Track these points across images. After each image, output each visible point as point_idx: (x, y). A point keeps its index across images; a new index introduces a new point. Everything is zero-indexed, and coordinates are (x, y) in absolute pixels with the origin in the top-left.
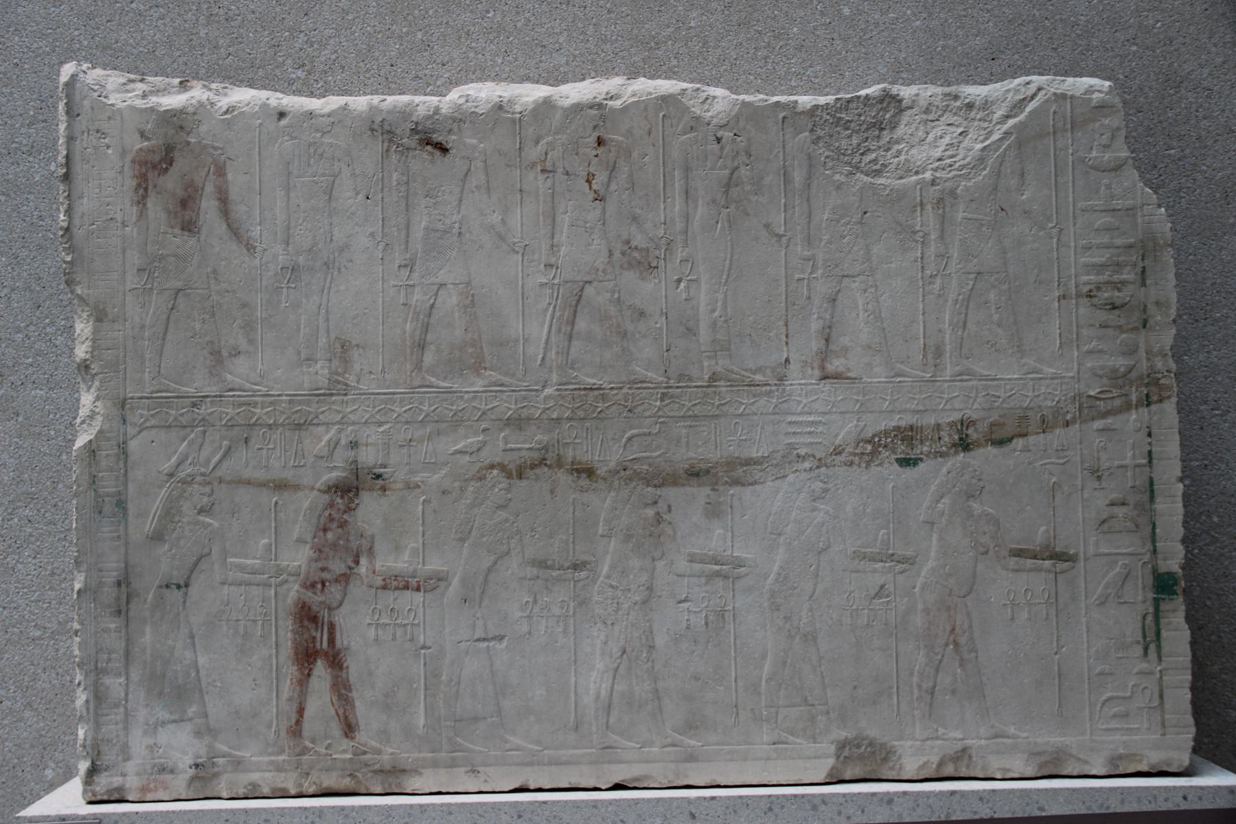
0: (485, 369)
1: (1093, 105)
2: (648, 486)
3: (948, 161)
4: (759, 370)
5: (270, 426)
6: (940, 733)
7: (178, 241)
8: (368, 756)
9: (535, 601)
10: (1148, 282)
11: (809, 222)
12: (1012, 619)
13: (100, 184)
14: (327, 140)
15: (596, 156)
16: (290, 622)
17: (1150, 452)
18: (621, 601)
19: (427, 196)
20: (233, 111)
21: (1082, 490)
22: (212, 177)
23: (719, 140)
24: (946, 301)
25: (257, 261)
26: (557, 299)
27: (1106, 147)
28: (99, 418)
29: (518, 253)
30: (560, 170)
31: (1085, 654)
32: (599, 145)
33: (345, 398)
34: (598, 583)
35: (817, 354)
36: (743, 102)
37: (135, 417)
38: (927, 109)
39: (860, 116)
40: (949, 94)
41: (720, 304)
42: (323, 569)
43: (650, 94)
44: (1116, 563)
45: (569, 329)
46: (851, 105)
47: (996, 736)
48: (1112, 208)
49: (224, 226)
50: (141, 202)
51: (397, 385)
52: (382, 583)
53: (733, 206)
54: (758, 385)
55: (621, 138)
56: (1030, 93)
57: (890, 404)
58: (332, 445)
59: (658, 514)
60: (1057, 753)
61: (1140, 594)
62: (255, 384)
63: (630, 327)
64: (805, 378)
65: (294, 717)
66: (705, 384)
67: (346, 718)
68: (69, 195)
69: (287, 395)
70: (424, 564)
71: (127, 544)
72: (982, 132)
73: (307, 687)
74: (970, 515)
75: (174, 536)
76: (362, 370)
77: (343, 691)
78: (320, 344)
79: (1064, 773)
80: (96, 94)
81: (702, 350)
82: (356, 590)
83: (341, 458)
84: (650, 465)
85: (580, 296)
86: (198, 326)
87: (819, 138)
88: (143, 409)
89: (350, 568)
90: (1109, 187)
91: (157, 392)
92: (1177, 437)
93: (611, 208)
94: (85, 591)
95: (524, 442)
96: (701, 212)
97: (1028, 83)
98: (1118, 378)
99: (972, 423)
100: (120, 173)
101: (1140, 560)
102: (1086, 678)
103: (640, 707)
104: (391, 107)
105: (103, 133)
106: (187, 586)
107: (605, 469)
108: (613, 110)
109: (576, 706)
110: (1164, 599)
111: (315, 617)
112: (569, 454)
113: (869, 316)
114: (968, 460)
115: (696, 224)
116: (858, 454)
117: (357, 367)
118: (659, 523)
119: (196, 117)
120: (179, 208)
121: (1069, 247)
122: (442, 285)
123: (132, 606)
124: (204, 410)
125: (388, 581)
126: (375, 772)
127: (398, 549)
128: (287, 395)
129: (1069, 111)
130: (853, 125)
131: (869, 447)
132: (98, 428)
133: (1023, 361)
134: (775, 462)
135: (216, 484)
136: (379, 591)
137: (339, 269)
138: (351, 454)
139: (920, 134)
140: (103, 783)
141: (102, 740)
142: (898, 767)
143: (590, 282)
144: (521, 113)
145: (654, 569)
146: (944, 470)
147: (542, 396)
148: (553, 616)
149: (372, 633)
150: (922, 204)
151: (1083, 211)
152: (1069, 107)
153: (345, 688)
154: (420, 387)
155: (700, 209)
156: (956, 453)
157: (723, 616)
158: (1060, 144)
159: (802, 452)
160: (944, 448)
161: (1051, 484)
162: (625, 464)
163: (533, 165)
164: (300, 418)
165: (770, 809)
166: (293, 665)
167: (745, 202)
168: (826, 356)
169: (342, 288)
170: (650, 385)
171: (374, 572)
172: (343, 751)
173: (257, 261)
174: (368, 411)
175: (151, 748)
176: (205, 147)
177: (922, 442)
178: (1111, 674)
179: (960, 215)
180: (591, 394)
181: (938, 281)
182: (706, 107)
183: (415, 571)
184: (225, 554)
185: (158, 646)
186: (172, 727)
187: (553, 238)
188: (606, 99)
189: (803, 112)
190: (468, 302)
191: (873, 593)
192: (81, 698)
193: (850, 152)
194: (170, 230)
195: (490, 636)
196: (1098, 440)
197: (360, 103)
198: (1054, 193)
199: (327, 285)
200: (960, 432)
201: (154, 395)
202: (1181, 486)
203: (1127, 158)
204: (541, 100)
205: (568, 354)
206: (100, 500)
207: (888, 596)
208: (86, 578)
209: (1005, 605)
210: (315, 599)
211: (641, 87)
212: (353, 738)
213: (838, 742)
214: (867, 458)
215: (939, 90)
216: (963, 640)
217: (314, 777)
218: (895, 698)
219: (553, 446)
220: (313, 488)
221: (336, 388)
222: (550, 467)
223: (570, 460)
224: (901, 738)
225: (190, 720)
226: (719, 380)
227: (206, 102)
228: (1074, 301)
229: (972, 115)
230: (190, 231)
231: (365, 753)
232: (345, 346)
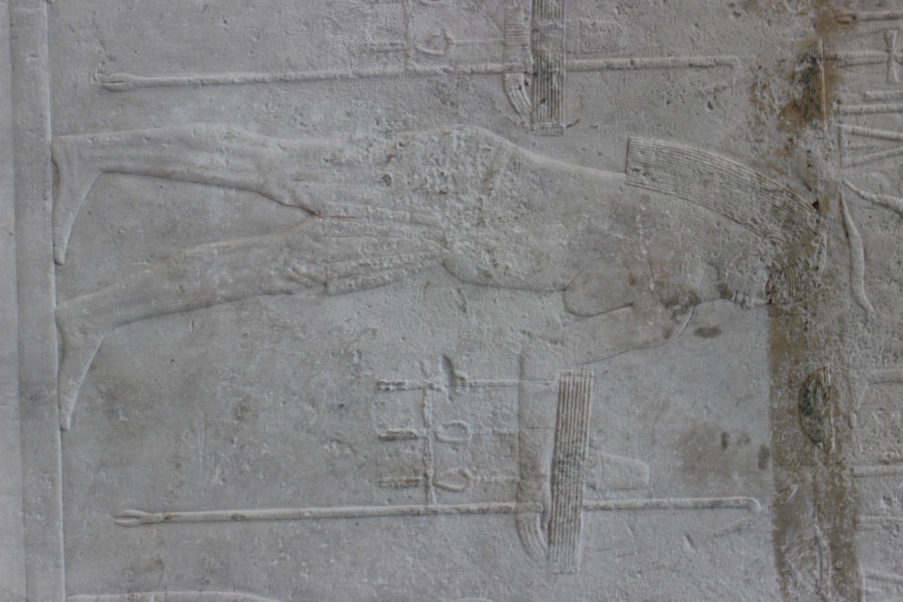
18: (451, 202)
34: (498, 138)
59: (695, 301)
84: (831, 276)
107: (818, 152)
109: (162, 85)
118: (667, 305)
145: (538, 291)
148: (407, 17)
162: (834, 203)
223: (842, 53)
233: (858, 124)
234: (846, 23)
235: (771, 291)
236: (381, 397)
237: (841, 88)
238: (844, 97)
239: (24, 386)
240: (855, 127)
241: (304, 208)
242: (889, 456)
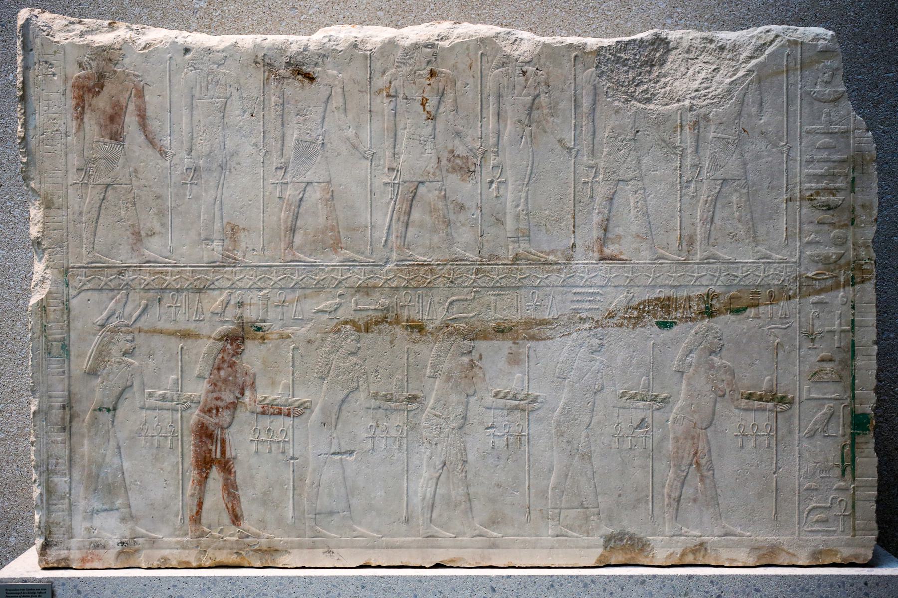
0: (341, 248)
1: (818, 50)
2: (465, 339)
3: (703, 92)
4: (552, 252)
5: (177, 290)
6: (683, 531)
7: (107, 147)
8: (250, 539)
9: (377, 426)
10: (856, 189)
11: (594, 138)
12: (742, 447)
13: (48, 104)
14: (221, 70)
15: (429, 85)
16: (192, 438)
17: (853, 321)
18: (442, 426)
19: (298, 114)
20: (149, 47)
21: (799, 349)
22: (133, 98)
23: (524, 73)
24: (699, 201)
25: (168, 163)
26: (397, 195)
27: (827, 83)
28: (49, 282)
29: (367, 159)
30: (401, 95)
31: (797, 474)
32: (431, 76)
33: (234, 269)
34: (426, 413)
35: (597, 241)
37: (75, 282)
38: (689, 49)
39: (635, 55)
40: (706, 39)
41: (523, 200)
42: (217, 399)
43: (472, 36)
44: (823, 405)
45: (406, 218)
46: (629, 47)
47: (726, 535)
48: (830, 131)
49: (143, 137)
50: (80, 117)
51: (274, 260)
52: (262, 409)
53: (534, 125)
54: (551, 264)
55: (448, 71)
56: (769, 39)
57: (653, 279)
58: (224, 305)
59: (472, 360)
60: (772, 548)
61: (840, 429)
62: (166, 258)
63: (453, 217)
64: (587, 259)
65: (195, 509)
67: (234, 510)
68: (25, 112)
69: (190, 266)
70: (293, 396)
71: (70, 377)
72: (731, 69)
73: (205, 487)
74: (712, 367)
75: (105, 372)
76: (247, 247)
77: (232, 490)
78: (215, 227)
79: (777, 563)
80: (45, 34)
81: (509, 235)
82: (242, 414)
83: (232, 313)
84: (466, 324)
85: (415, 193)
86: (123, 213)
87: (603, 72)
88: (81, 275)
89: (238, 398)
90: (828, 114)
91: (92, 263)
92: (874, 310)
93: (440, 124)
94: (39, 412)
95: (370, 304)
96: (509, 129)
97: (768, 31)
98: (829, 263)
99: (715, 296)
100: (63, 94)
101: (842, 403)
102: (797, 492)
103: (456, 506)
104: (270, 45)
105: (51, 64)
106: (115, 409)
108: (443, 49)
109: (407, 506)
110: (859, 434)
111: (211, 434)
112: (405, 314)
113: (638, 212)
114: (712, 324)
115: (505, 139)
116: (627, 318)
117: (243, 245)
118: (473, 368)
119: (121, 52)
120: (108, 122)
121: (796, 161)
122: (309, 184)
123: (74, 424)
124: (128, 277)
125: (266, 408)
126: (256, 551)
127: (274, 384)
128: (190, 266)
129: (799, 54)
130: (629, 62)
131: (636, 313)
132: (47, 290)
133: (757, 249)
134: (562, 323)
135: (136, 333)
136: (259, 415)
137: (230, 170)
138: (239, 311)
139: (682, 69)
140: (54, 554)
141: (53, 523)
142: (650, 555)
143: (423, 183)
145: (468, 403)
146: (693, 332)
147: (385, 270)
148: (391, 437)
149: (253, 447)
150: (681, 126)
151: (808, 133)
152: (799, 51)
153: (233, 488)
154: (291, 261)
155: (509, 127)
156: (703, 319)
157: (520, 440)
158: (792, 80)
159: (584, 315)
160: (693, 315)
161: (776, 344)
162: (447, 322)
163: (380, 91)
164: (200, 284)
165: (552, 586)
166: (194, 470)
168: (604, 242)
169: (233, 185)
170: (467, 262)
171: (256, 402)
172: (232, 534)
173: (168, 163)
174: (251, 279)
175: (88, 530)
176: (128, 75)
177: (676, 310)
178: (816, 490)
179: (712, 135)
181: (693, 185)
183: (287, 400)
184: (143, 385)
185: (93, 454)
186: (104, 514)
187: (394, 148)
188: (437, 40)
189: (590, 52)
190: (328, 196)
191: (635, 424)
192: (37, 492)
193: (626, 84)
194: (101, 139)
195: (343, 451)
196: (813, 311)
197: (247, 41)
198: (785, 118)
199: (221, 182)
200: (706, 303)
201: (90, 265)
202: (876, 347)
203: (843, 92)
204: (387, 41)
206: (49, 344)
207: (647, 427)
208: (39, 403)
209: (736, 435)
210: (210, 421)
211: (465, 31)
212: (239, 526)
213: (606, 536)
214: (633, 321)
215: (699, 35)
216: (703, 462)
217: (210, 552)
218: (650, 503)
219: (393, 307)
220: (209, 337)
221: (228, 262)
222: (390, 324)
223: (406, 318)
224: (653, 534)
225: (117, 509)
226: (521, 259)
227: (129, 41)
228: (798, 203)
229: (724, 55)
230: (116, 140)
231: (248, 536)
232: (235, 230)
235: (470, 340)
236: (496, 447)
239: (490, 547)
241: (443, 467)
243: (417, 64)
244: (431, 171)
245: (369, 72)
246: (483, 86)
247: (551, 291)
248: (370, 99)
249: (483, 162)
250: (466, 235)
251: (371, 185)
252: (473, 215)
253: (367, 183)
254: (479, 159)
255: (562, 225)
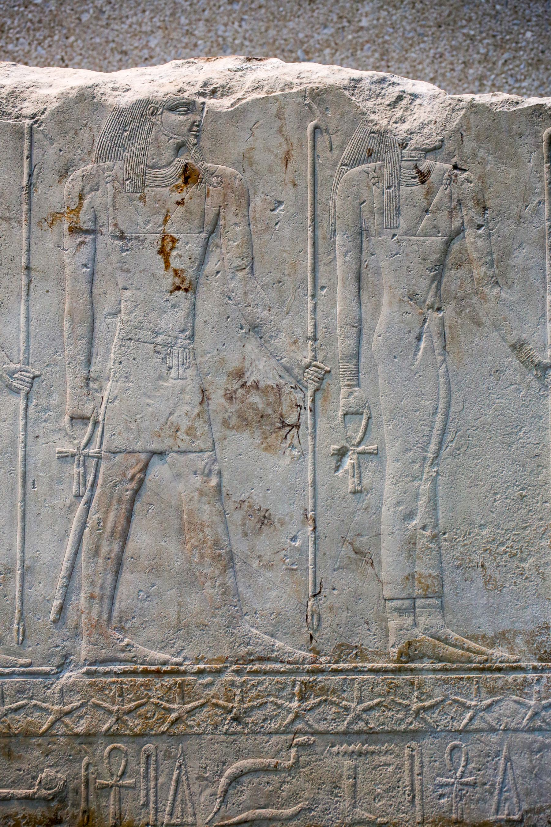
26: (93, 486)
29: (17, 391)
32: (186, 182)
36: (472, 105)
41: (422, 501)
43: (290, 85)
45: (116, 547)
53: (450, 307)
54: (499, 670)
55: (230, 170)
66: (391, 665)
81: (387, 593)
85: (141, 482)
95: (14, 784)
108: (216, 115)
143: (161, 454)
144: (33, 117)
147: (57, 687)
155: (385, 311)
167: (475, 299)
170: (278, 666)
180: (158, 682)
182: (399, 113)
187: (89, 362)
188: (202, 94)
204: (73, 94)
205: (112, 598)
211: (274, 73)
219: (77, 791)
226: (421, 658)
233: (165, 811)
234: (88, 817)
237: (136, 823)
238: (144, 821)
240: (166, 812)
242: (409, 795)
243: (151, 151)
244: (184, 425)
245: (26, 171)
246: (319, 207)
247: (501, 744)
248: (29, 238)
249: (319, 402)
250: (274, 593)
251: (25, 459)
252: (294, 539)
253: (15, 454)
254: (309, 393)
255: (526, 565)
